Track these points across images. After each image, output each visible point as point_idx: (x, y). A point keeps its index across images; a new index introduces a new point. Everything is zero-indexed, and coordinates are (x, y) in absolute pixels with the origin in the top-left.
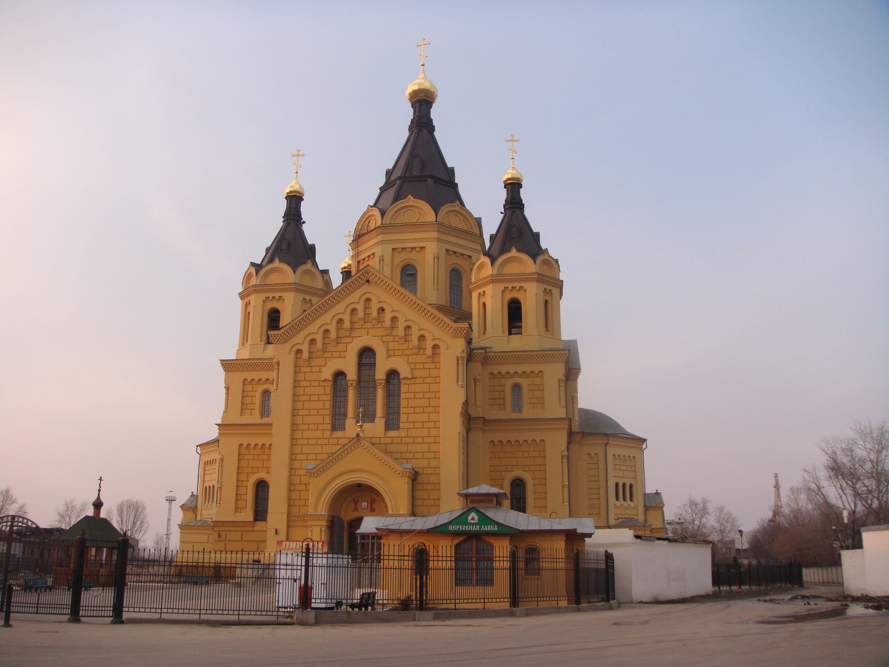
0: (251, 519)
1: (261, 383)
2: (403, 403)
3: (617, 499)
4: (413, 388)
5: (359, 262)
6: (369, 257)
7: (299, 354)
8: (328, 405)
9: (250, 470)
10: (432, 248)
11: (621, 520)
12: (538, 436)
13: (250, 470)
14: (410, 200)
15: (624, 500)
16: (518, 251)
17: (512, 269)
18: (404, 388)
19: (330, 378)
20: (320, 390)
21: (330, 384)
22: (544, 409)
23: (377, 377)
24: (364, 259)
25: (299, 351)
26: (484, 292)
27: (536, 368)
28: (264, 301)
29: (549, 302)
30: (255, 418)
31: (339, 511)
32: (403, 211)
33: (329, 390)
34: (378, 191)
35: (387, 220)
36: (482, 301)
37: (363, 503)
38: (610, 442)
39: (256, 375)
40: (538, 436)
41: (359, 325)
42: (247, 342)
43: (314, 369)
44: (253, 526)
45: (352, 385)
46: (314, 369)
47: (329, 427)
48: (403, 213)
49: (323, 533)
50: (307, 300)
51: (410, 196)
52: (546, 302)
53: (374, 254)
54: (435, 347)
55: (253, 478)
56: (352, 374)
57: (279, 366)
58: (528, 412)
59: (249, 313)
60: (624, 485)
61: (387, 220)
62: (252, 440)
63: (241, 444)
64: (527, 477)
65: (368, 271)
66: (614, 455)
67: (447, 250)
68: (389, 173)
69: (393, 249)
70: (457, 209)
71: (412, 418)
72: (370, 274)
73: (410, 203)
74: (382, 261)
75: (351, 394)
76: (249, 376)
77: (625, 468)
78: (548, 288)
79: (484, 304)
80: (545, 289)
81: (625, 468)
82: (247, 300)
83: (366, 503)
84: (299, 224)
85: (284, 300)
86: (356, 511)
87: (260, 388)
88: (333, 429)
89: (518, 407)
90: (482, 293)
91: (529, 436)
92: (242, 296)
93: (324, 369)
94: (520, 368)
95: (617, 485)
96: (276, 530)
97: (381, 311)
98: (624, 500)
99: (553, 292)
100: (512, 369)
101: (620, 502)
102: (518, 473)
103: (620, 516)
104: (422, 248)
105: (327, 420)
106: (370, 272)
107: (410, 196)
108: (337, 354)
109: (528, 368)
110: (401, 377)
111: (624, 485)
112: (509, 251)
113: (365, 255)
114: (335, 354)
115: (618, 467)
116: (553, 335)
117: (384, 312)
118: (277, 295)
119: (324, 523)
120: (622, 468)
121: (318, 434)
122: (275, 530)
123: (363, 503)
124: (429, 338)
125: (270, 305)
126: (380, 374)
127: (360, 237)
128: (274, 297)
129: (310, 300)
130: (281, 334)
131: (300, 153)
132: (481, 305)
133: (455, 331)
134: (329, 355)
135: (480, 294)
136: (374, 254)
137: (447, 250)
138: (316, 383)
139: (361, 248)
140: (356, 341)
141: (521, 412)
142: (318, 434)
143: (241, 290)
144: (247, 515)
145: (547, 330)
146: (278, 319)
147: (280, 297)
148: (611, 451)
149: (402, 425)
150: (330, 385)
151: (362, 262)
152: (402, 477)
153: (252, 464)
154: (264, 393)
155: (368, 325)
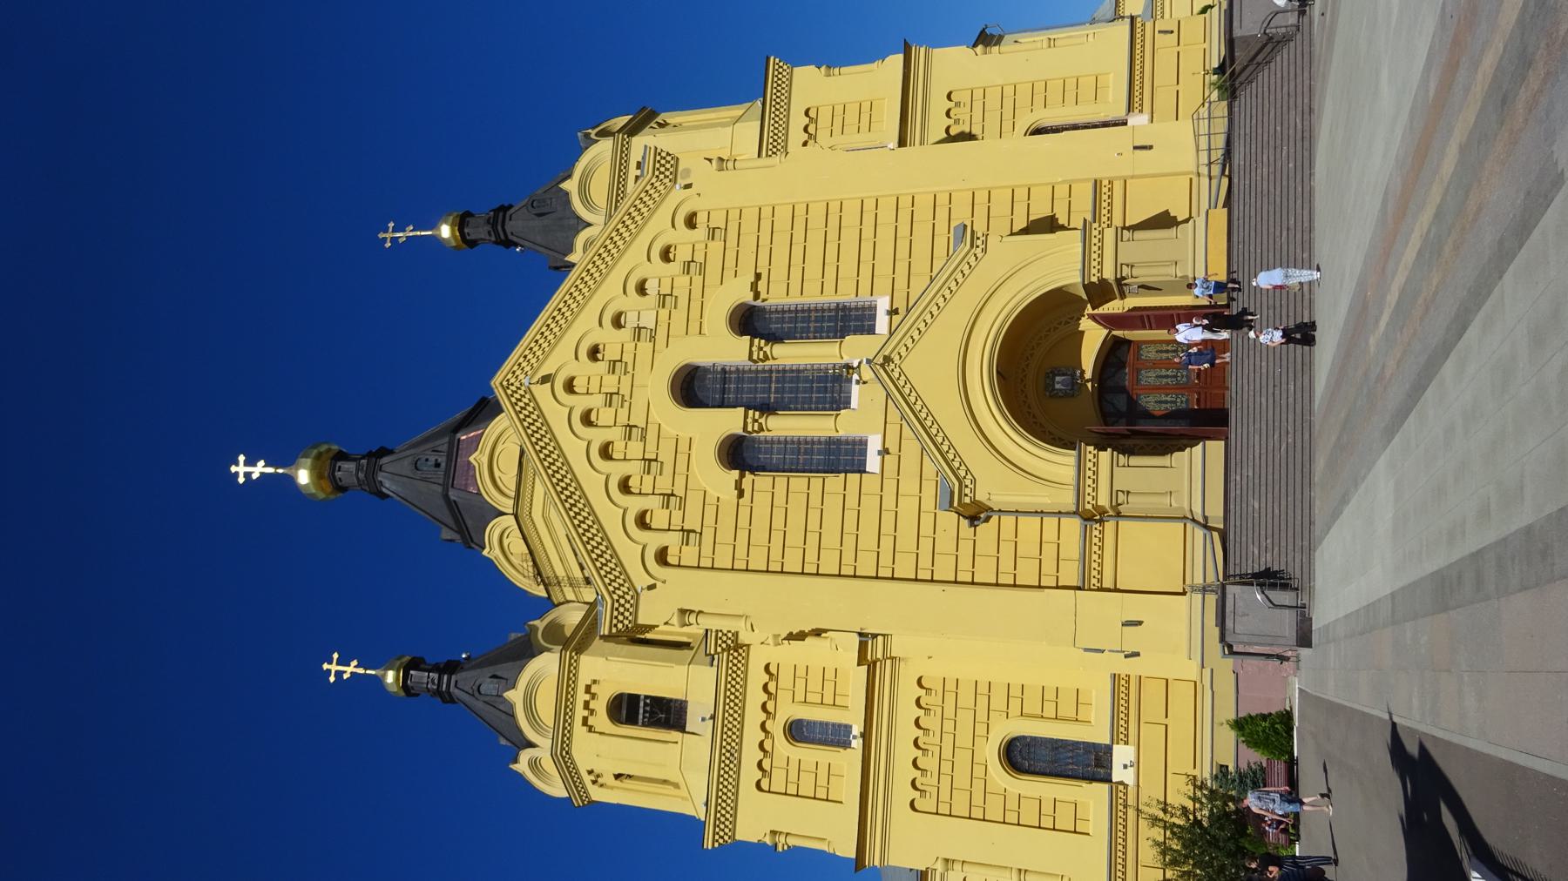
0: (1106, 787)
1: (768, 746)
7: (670, 559)
8: (799, 482)
9: (978, 784)
13: (978, 784)
14: (479, 459)
16: (569, 176)
17: (600, 189)
19: (736, 474)
20: (762, 500)
21: (749, 477)
28: (590, 729)
30: (848, 761)
32: (497, 473)
33: (763, 481)
35: (507, 505)
37: (1057, 386)
39: (750, 755)
41: (622, 407)
42: (676, 786)
43: (709, 520)
44: (1126, 786)
45: (756, 421)
46: (709, 520)
47: (853, 478)
48: (501, 474)
49: (1134, 460)
51: (471, 459)
54: (691, 222)
55: (1000, 777)
56: (730, 421)
57: (692, 611)
59: (618, 776)
61: (507, 505)
62: (903, 773)
63: (912, 805)
65: (505, 383)
72: (512, 381)
73: (485, 460)
76: (749, 774)
82: (587, 779)
83: (1058, 379)
85: (595, 682)
87: (782, 747)
88: (861, 470)
93: (713, 494)
105: (834, 481)
107: (471, 459)
108: (682, 459)
110: (748, 297)
112: (567, 194)
114: (681, 467)
118: (582, 697)
119: (1105, 456)
121: (871, 504)
123: (1057, 386)
124: (669, 237)
125: (601, 720)
127: (539, 574)
128: (586, 705)
130: (612, 598)
133: (662, 177)
134: (680, 481)
138: (744, 513)
139: (560, 572)
142: (871, 504)
144: (1093, 796)
147: (588, 689)
149: (864, 296)
150: (753, 476)
152: (985, 251)
153: (962, 780)
154: (793, 738)
155: (625, 391)
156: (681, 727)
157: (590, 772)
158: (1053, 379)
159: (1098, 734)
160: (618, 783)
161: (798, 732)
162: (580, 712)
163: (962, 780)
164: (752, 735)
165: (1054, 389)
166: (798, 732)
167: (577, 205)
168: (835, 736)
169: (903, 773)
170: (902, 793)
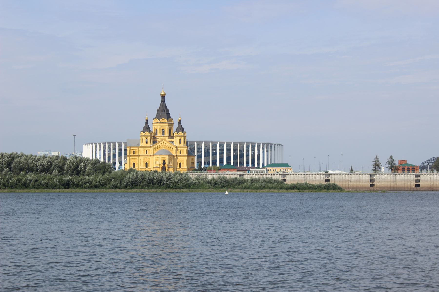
10: (167, 127)
27: (183, 148)
34: (156, 114)
35: (160, 122)
39: (145, 148)
40: (183, 157)
58: (181, 154)
59: (142, 139)
64: (181, 162)
68: (158, 110)
76: (144, 148)
89: (180, 153)
94: (181, 148)
100: (180, 148)
109: (182, 148)
125: (146, 138)
153: (145, 160)
156: (146, 143)
161: (147, 151)
162: (146, 137)
163: (145, 160)
164: (146, 148)
166: (147, 151)
167: (179, 133)
168: (147, 153)
169: (145, 157)
170: (144, 157)
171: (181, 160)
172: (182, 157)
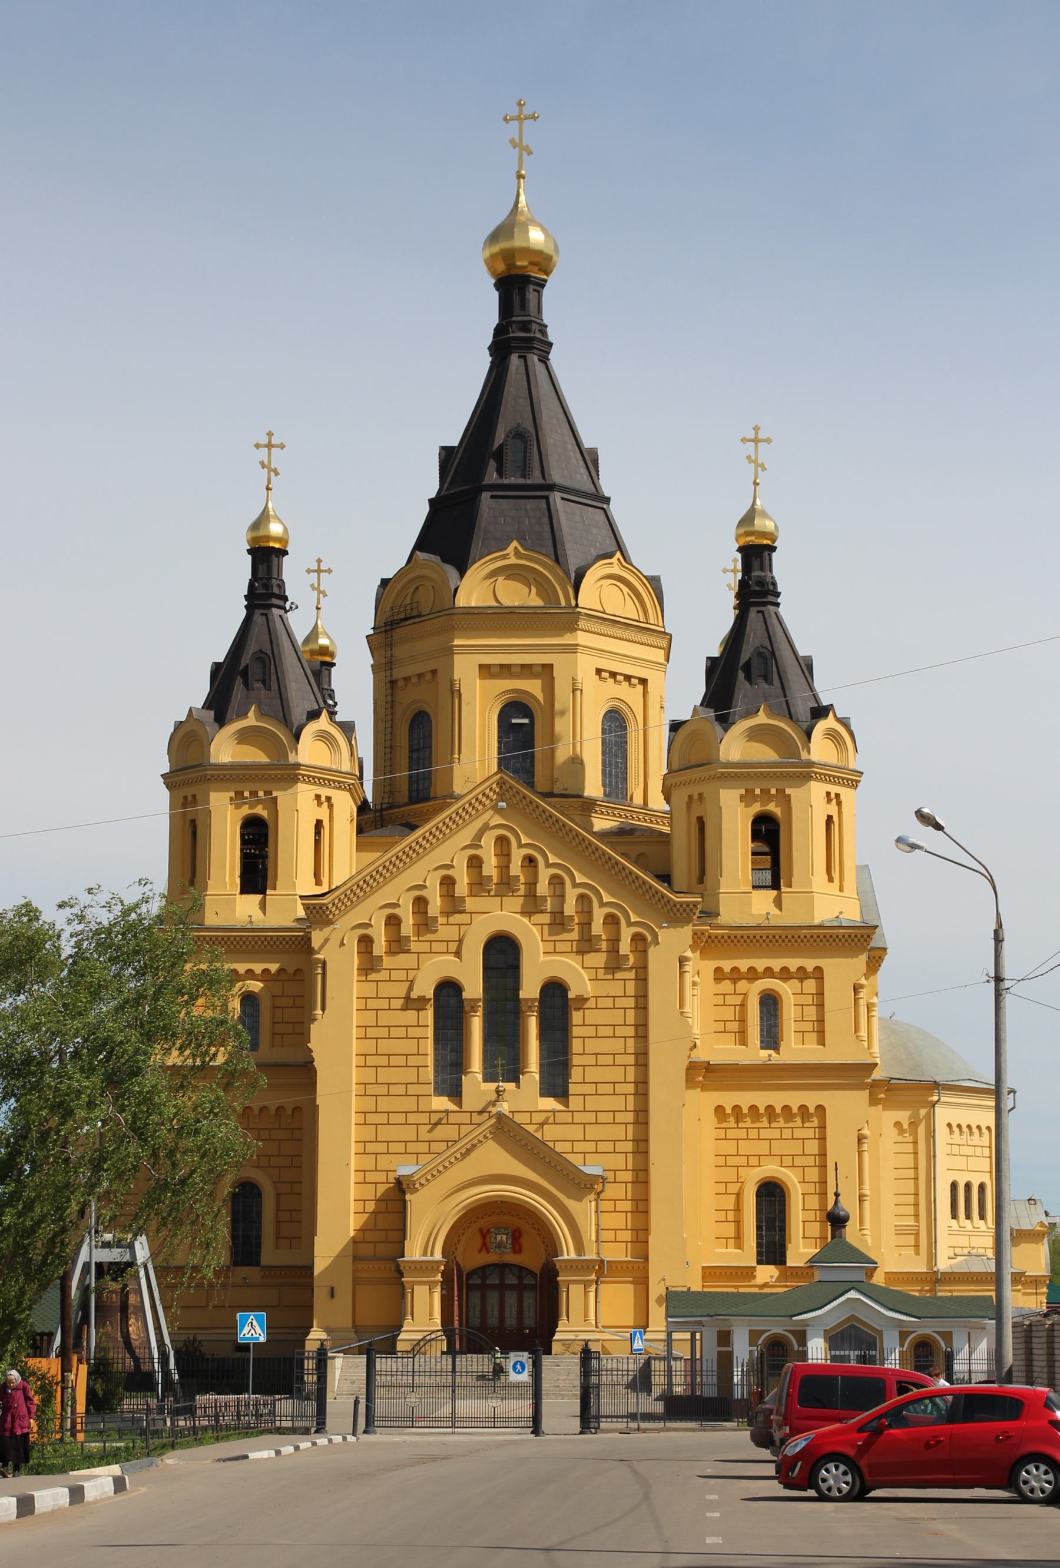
2: (576, 1046)
3: (954, 1215)
4: (591, 1016)
5: (393, 683)
6: (420, 676)
11: (959, 1259)
12: (811, 1099)
15: (968, 1216)
18: (576, 1017)
22: (824, 1045)
23: (523, 994)
24: (407, 679)
25: (366, 941)
26: (700, 795)
29: (836, 819)
31: (454, 1253)
36: (696, 812)
37: (499, 1237)
38: (943, 1099)
40: (811, 1099)
42: (192, 883)
50: (323, 799)
51: (515, 544)
52: (829, 819)
53: (434, 672)
54: (637, 938)
56: (474, 987)
60: (968, 1186)
64: (791, 1179)
66: (949, 1125)
67: (599, 671)
69: (480, 665)
70: (616, 570)
71: (592, 1074)
74: (456, 694)
75: (476, 1025)
77: (970, 1151)
78: (834, 789)
79: (701, 821)
80: (828, 794)
81: (970, 1151)
82: (189, 791)
83: (504, 1237)
84: (282, 612)
86: (484, 1251)
89: (771, 1039)
90: (696, 797)
91: (795, 1099)
92: (170, 780)
95: (954, 1186)
96: (332, 1289)
97: (527, 863)
98: (968, 1216)
99: (842, 797)
101: (958, 1222)
102: (771, 1169)
103: (958, 1251)
104: (544, 666)
106: (504, 783)
107: (515, 544)
111: (968, 1186)
113: (411, 670)
114: (436, 947)
115: (955, 1149)
116: (841, 889)
117: (532, 864)
120: (966, 1150)
122: (330, 1289)
126: (530, 989)
129: (329, 799)
131: (275, 441)
132: (694, 821)
135: (690, 797)
136: (434, 672)
137: (599, 671)
139: (401, 651)
140: (478, 919)
141: (776, 1048)
143: (166, 769)
145: (831, 879)
146: (262, 840)
148: (943, 1115)
149: (572, 1089)
151: (401, 683)
157: (194, 796)
158: (503, 1234)
159: (269, 1255)
160: (188, 823)
165: (496, 1234)
171: (778, 1147)
172: (795, 1099)
